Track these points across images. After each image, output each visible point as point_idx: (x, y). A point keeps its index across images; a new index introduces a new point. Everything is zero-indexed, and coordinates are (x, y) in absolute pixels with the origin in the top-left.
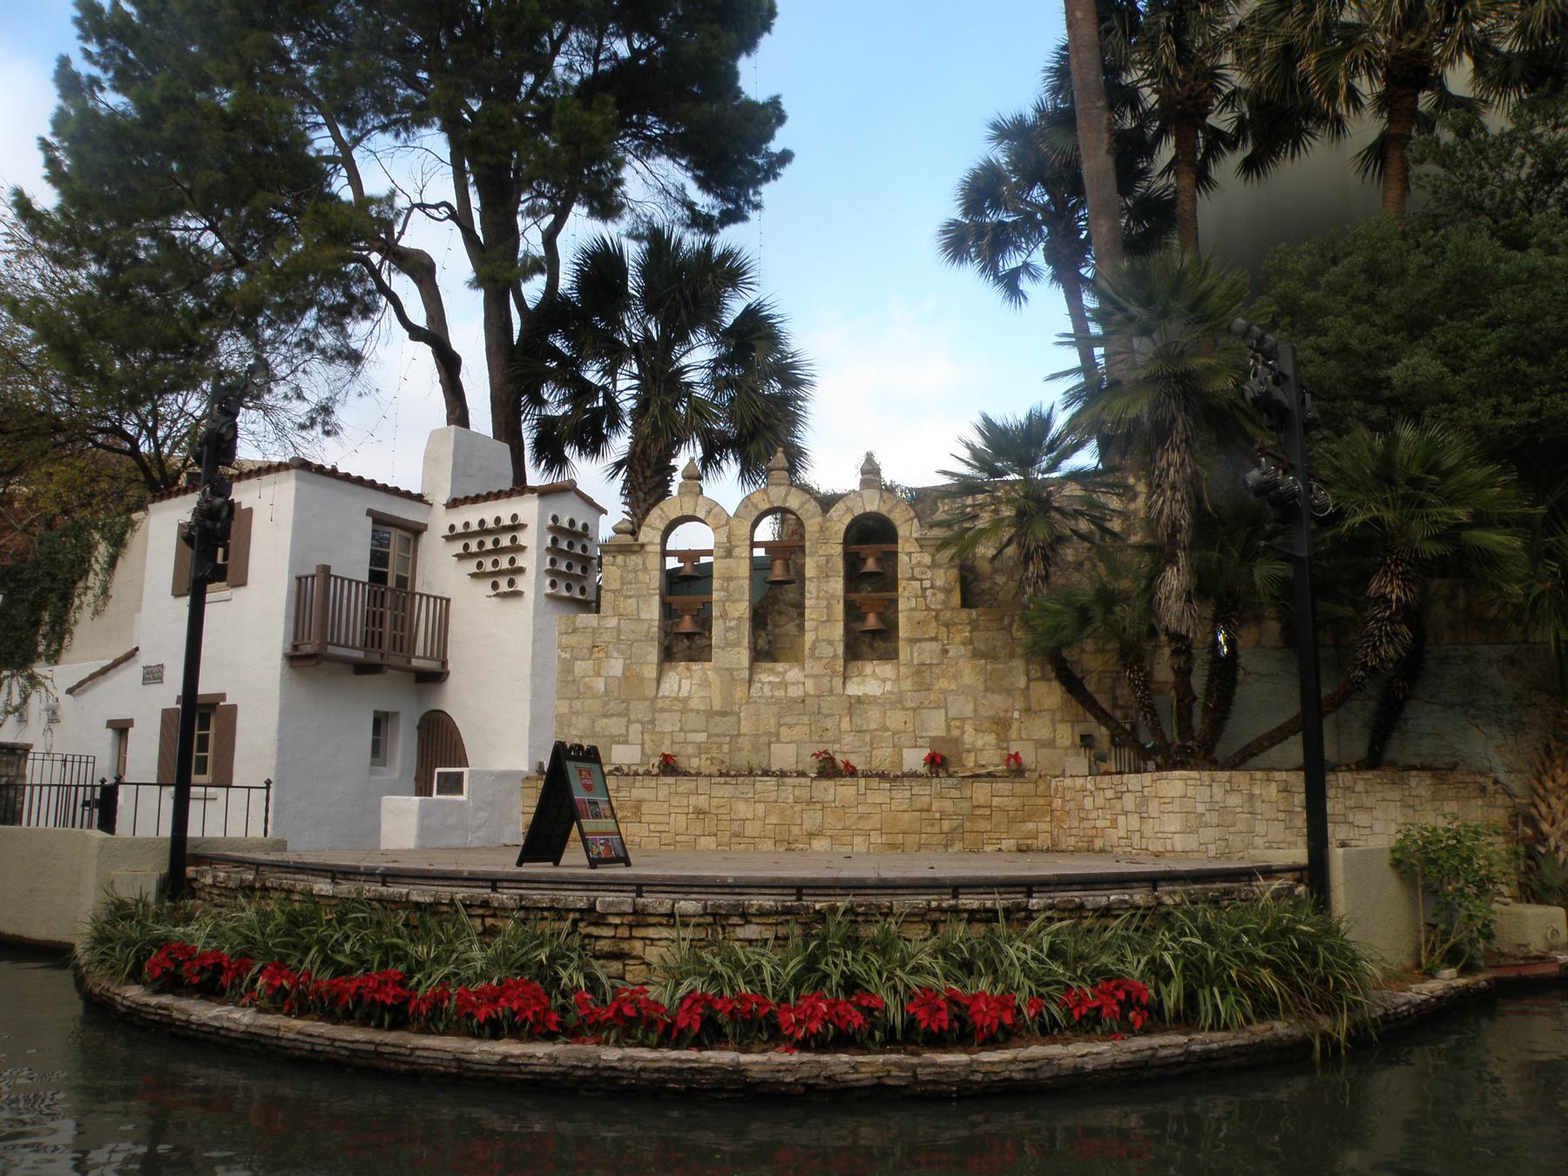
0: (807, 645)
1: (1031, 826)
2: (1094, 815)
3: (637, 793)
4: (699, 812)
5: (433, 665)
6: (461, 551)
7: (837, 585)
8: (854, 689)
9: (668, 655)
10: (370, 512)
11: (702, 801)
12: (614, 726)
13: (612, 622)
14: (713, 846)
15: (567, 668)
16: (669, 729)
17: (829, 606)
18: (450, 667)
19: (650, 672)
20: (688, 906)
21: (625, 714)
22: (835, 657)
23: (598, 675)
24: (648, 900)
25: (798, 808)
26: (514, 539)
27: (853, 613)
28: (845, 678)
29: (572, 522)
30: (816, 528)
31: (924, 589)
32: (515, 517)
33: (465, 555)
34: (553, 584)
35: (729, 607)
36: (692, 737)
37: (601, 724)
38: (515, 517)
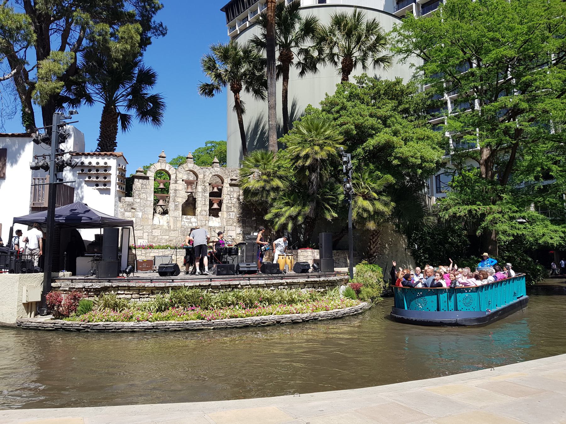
13: (138, 200)
17: (205, 200)
22: (206, 215)
23: (133, 217)
35: (176, 199)
36: (164, 237)
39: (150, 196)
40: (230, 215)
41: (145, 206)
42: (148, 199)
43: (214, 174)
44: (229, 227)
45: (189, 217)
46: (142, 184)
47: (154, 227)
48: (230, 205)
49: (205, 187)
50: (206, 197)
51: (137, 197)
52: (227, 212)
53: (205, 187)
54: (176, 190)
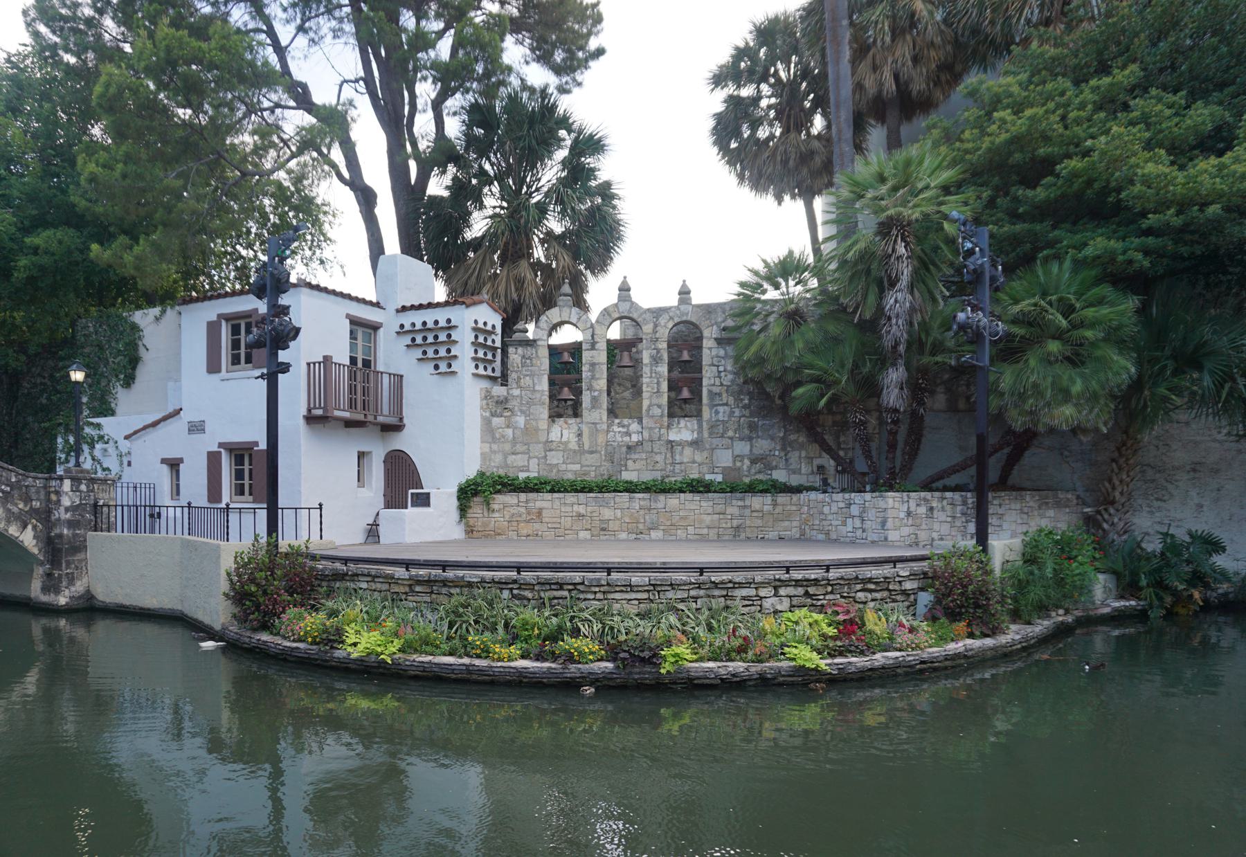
0: (645, 407)
1: (787, 523)
2: (830, 517)
3: (539, 504)
4: (580, 515)
5: (392, 420)
6: (409, 342)
7: (663, 369)
8: (673, 436)
9: (555, 416)
10: (348, 316)
11: (581, 509)
12: (519, 460)
13: (516, 392)
14: (589, 537)
15: (487, 423)
16: (555, 462)
17: (658, 383)
18: (405, 421)
19: (543, 425)
20: (636, 578)
21: (527, 452)
22: (662, 416)
23: (508, 427)
24: (614, 576)
25: (642, 512)
26: (449, 336)
27: (673, 386)
28: (669, 427)
29: (485, 324)
30: (650, 331)
31: (719, 372)
32: (449, 321)
33: (413, 345)
34: (477, 367)
35: (594, 384)
36: (571, 467)
37: (511, 458)
38: (449, 321)
39: (540, 381)
40: (717, 413)
41: (531, 402)
42: (537, 388)
43: (677, 320)
44: (716, 441)
45: (626, 422)
46: (523, 357)
47: (548, 446)
48: (716, 390)
49: (658, 351)
50: (659, 375)
51: (514, 385)
52: (712, 406)
53: (658, 352)
54: (593, 365)
